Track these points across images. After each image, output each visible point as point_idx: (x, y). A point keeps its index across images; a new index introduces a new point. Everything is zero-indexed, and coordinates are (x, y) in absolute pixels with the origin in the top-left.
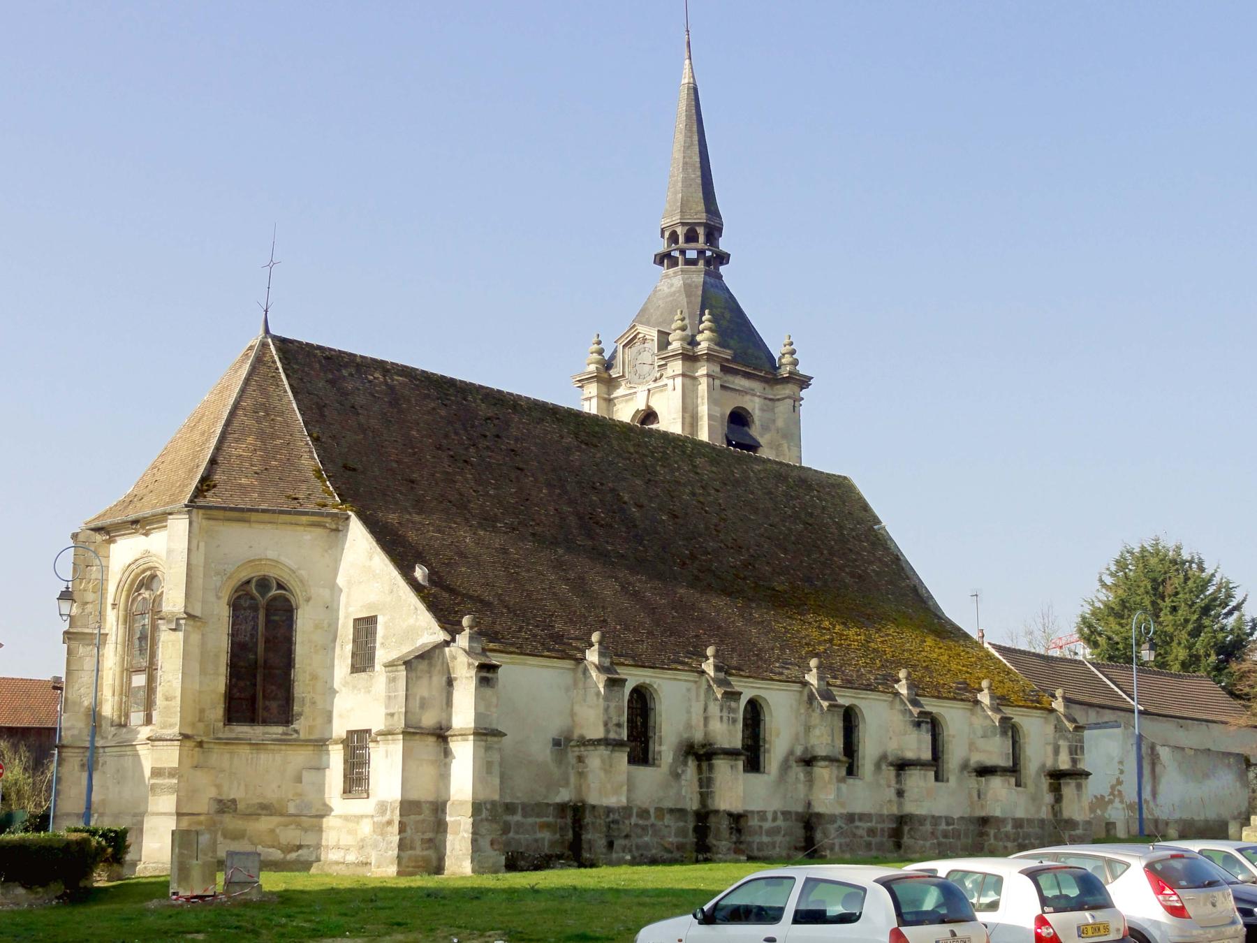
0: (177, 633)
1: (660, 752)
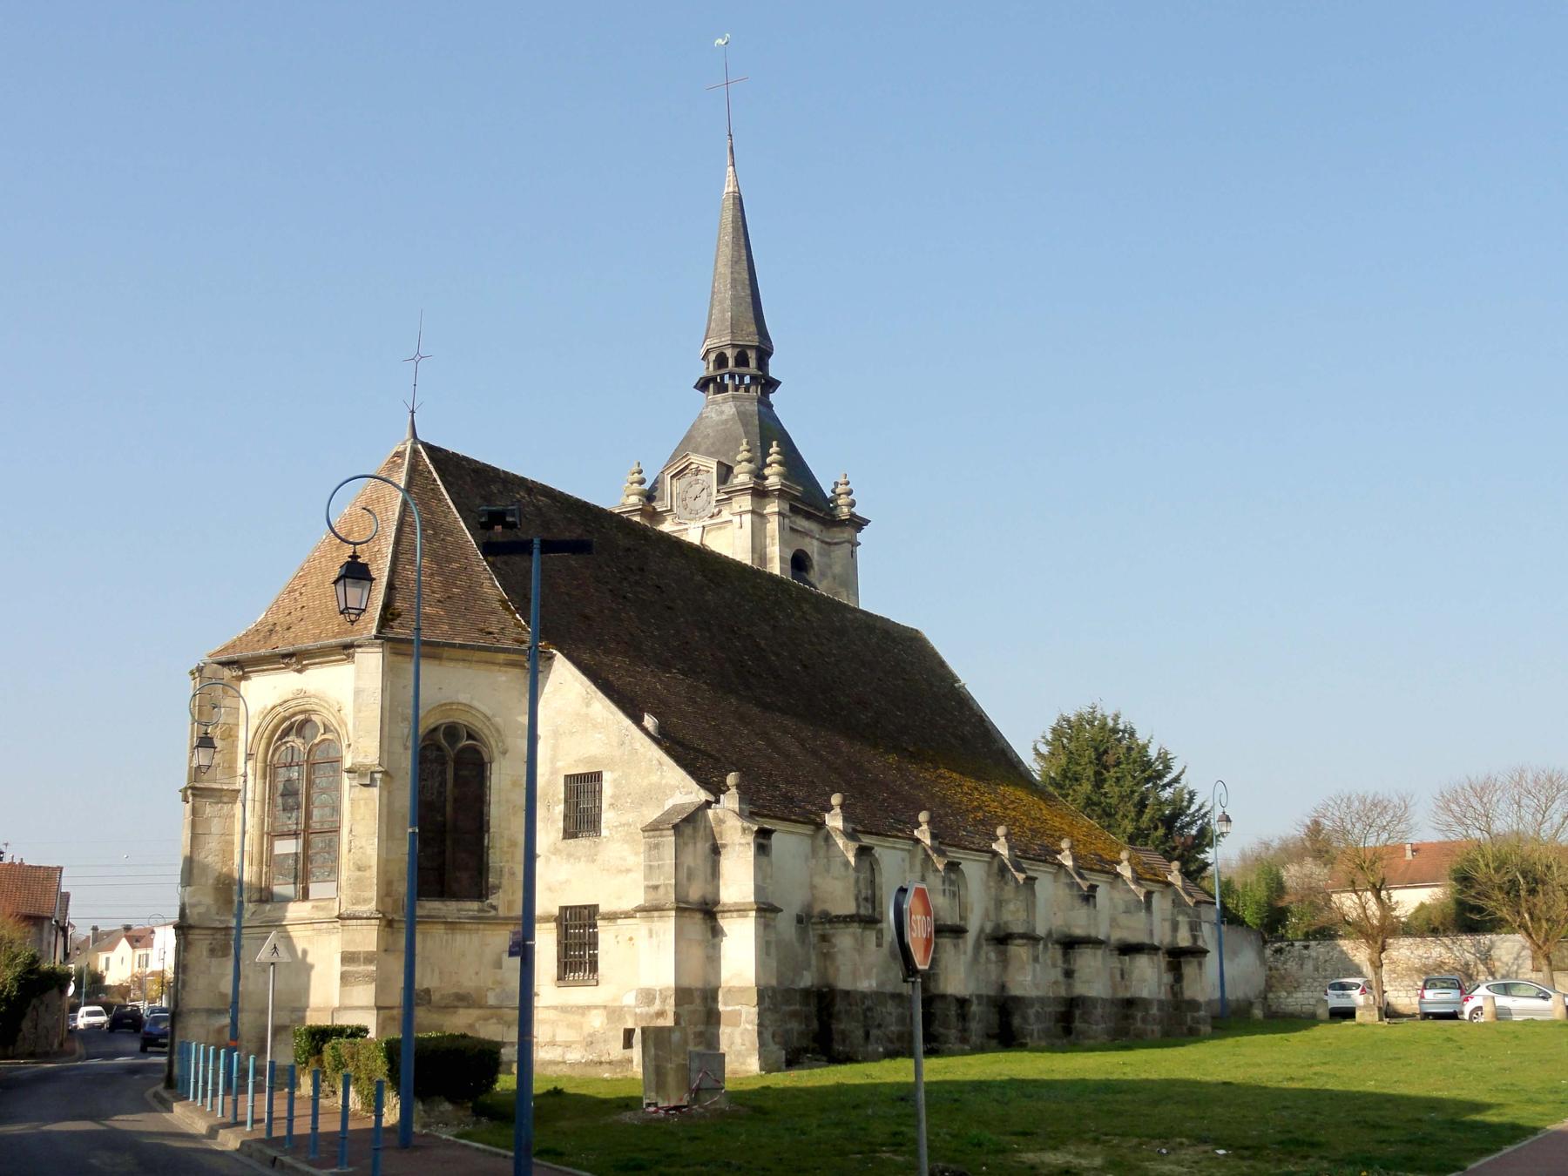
0: (371, 789)
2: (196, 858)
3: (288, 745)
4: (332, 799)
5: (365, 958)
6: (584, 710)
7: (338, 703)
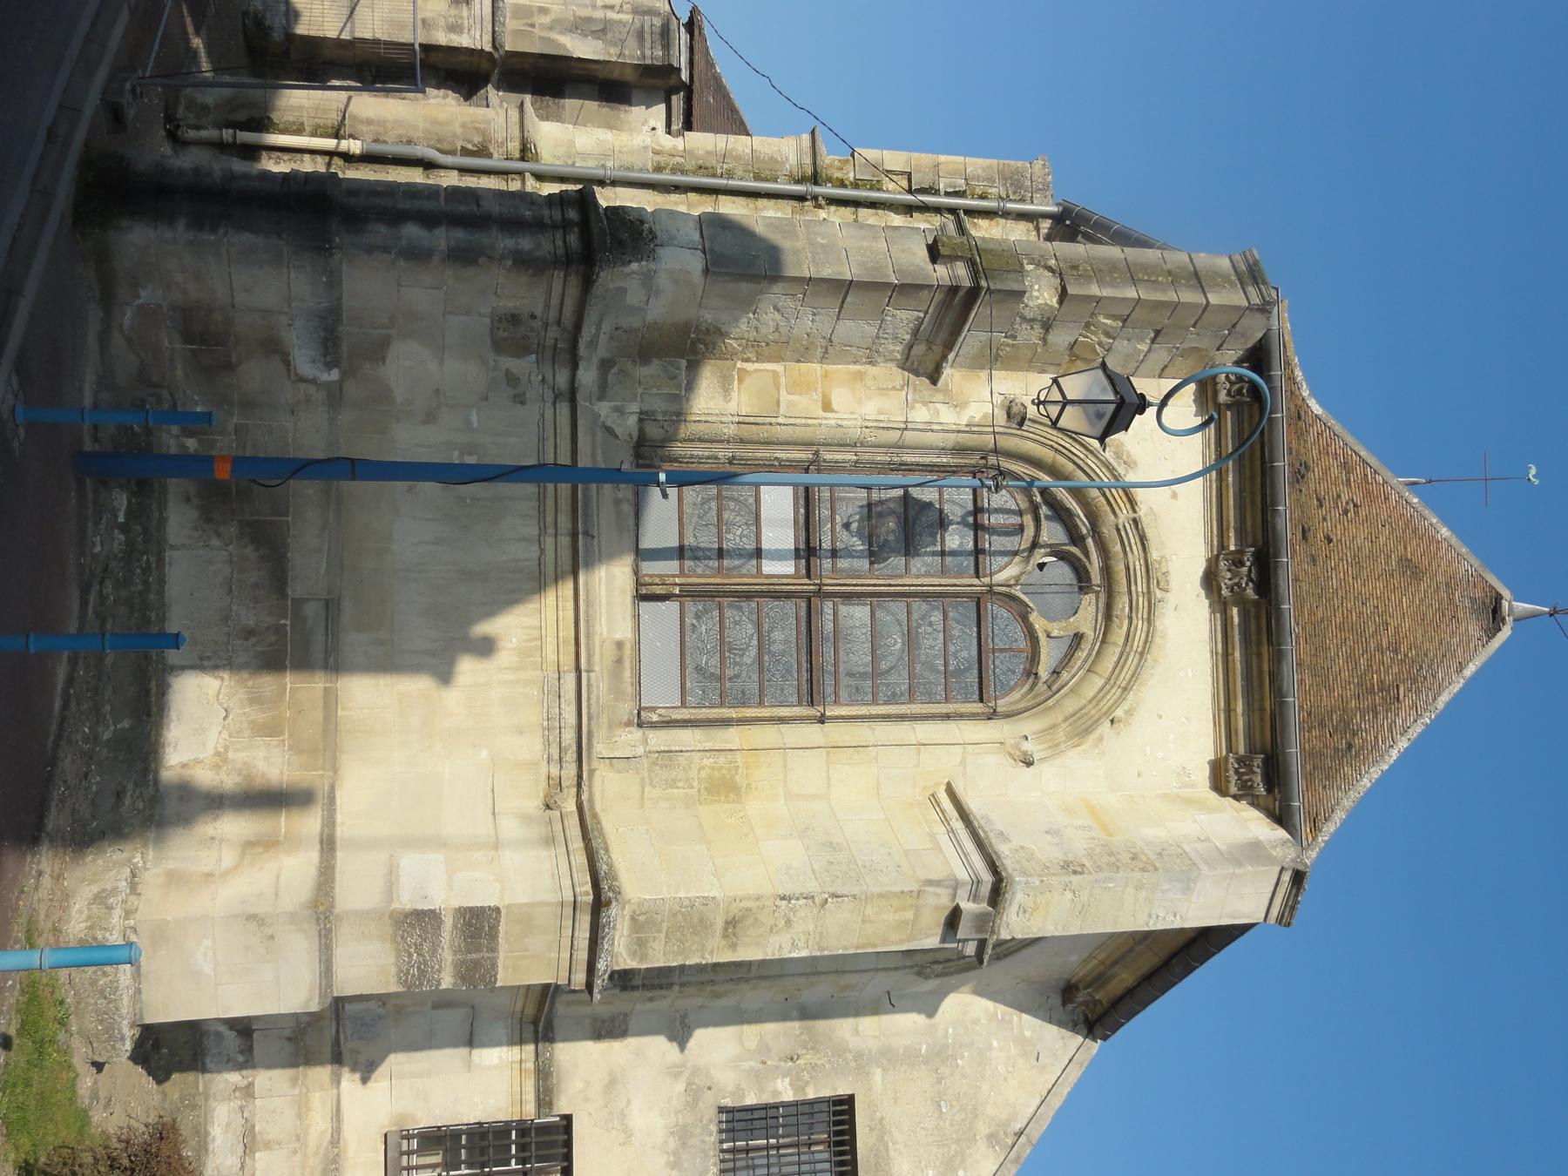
0: (939, 930)
2: (778, 288)
3: (1028, 520)
4: (888, 672)
5: (477, 964)
6: (983, 1129)
7: (1129, 713)
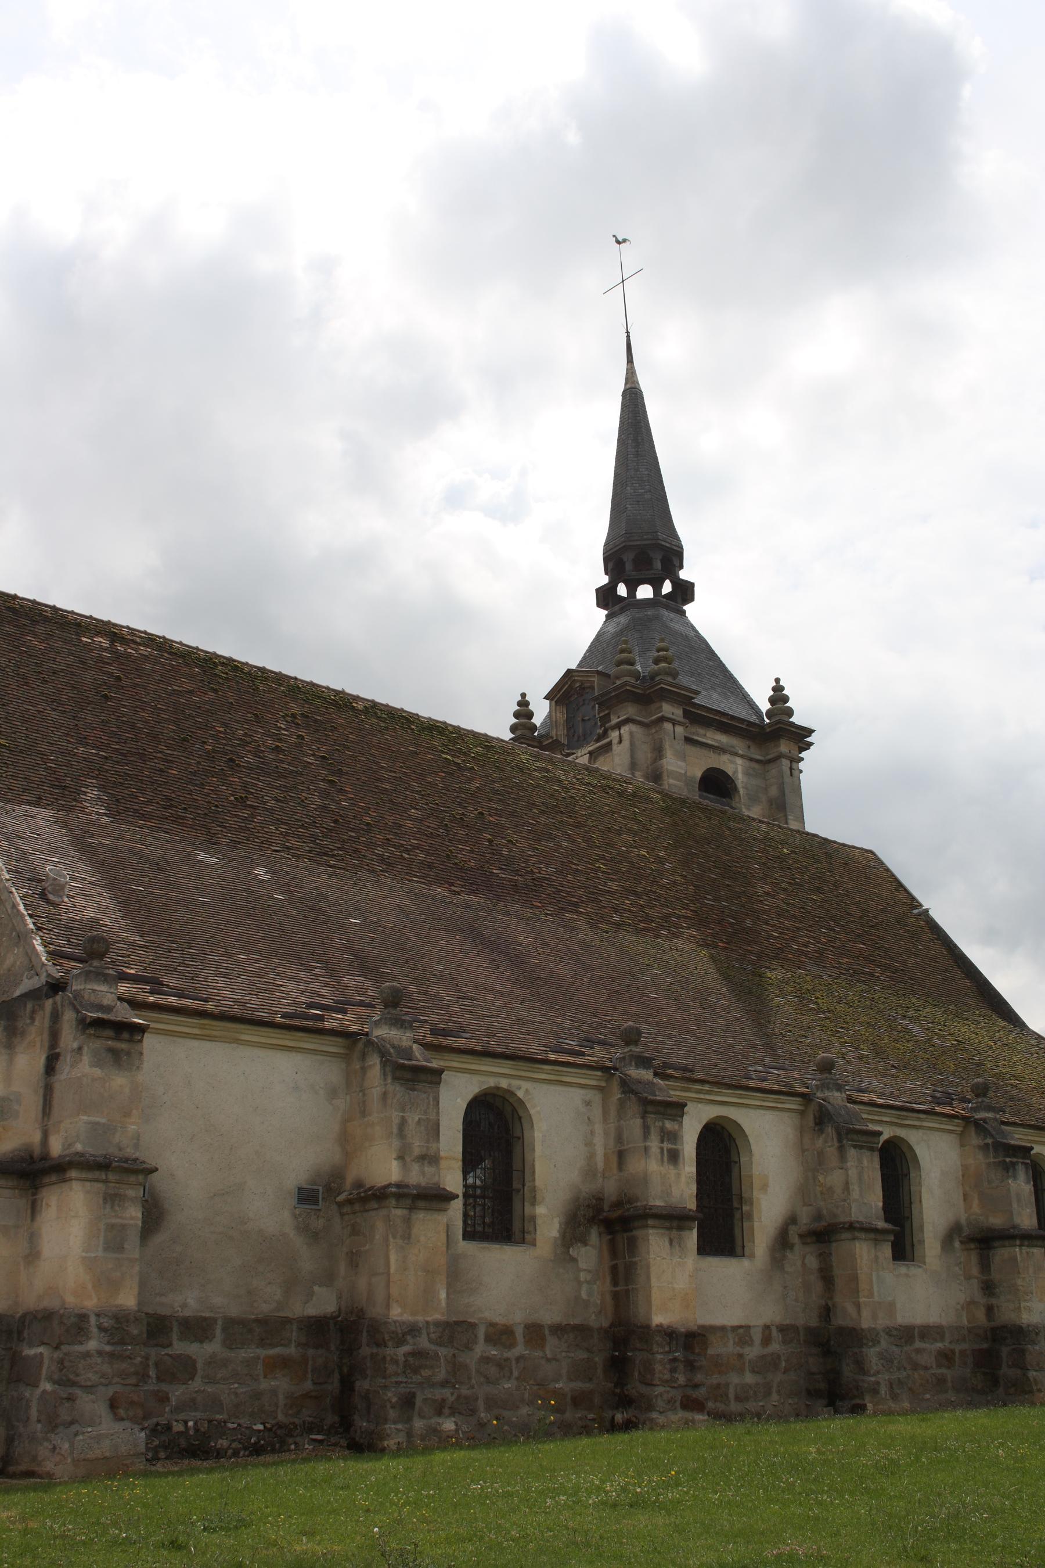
1: (533, 1218)
